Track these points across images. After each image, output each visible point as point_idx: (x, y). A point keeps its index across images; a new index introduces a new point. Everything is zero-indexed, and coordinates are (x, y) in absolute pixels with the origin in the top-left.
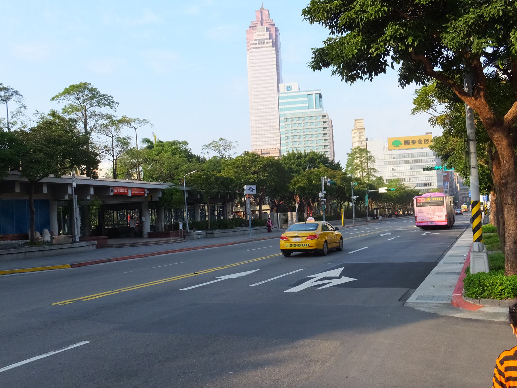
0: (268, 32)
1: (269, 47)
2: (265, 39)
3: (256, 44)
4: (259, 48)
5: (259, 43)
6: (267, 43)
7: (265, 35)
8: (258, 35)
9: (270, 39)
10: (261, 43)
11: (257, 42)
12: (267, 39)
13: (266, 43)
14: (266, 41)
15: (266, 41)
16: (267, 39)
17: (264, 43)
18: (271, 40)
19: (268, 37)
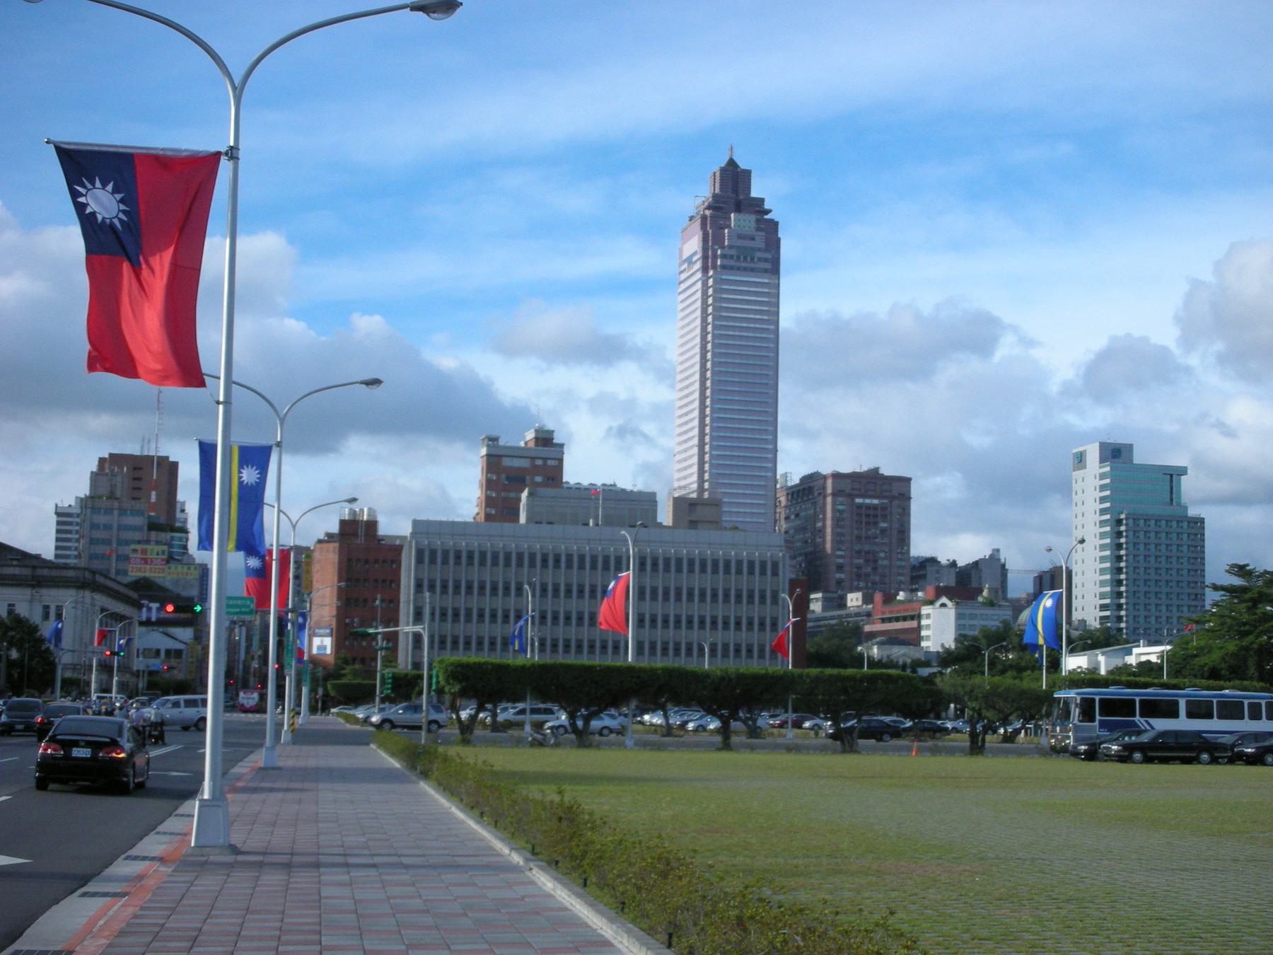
0: (763, 234)
1: (766, 271)
2: (752, 249)
3: (731, 257)
4: (739, 269)
5: (738, 257)
6: (759, 259)
7: (753, 239)
8: (740, 237)
9: (767, 250)
10: (745, 258)
11: (733, 252)
12: (759, 250)
13: (756, 259)
14: (759, 254)
15: (759, 254)
16: (759, 250)
17: (752, 259)
18: (769, 256)
19: (762, 245)
